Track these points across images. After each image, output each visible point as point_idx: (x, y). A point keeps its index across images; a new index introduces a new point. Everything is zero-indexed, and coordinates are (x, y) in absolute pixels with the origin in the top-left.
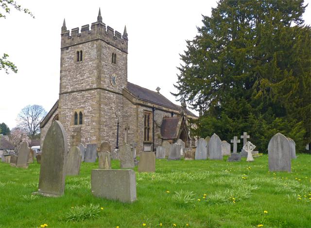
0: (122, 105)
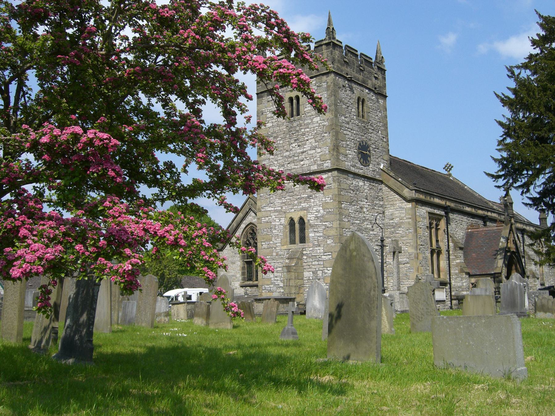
0: (381, 203)
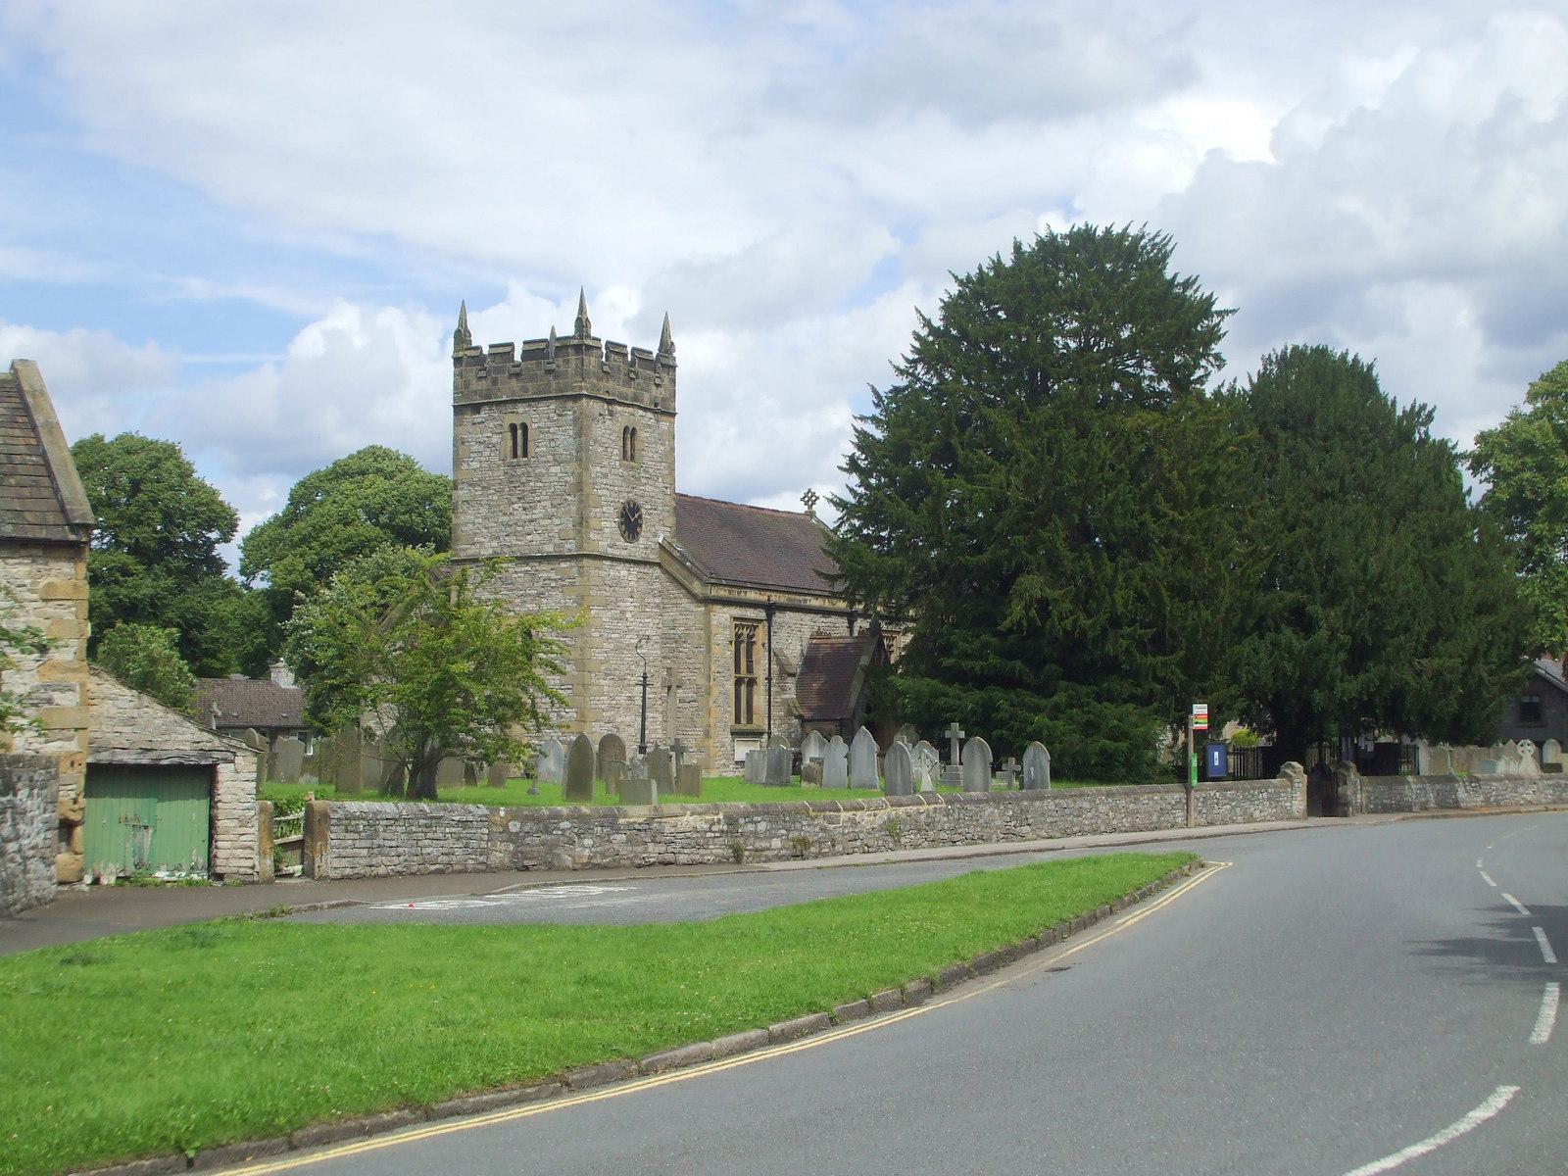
0: (657, 601)
